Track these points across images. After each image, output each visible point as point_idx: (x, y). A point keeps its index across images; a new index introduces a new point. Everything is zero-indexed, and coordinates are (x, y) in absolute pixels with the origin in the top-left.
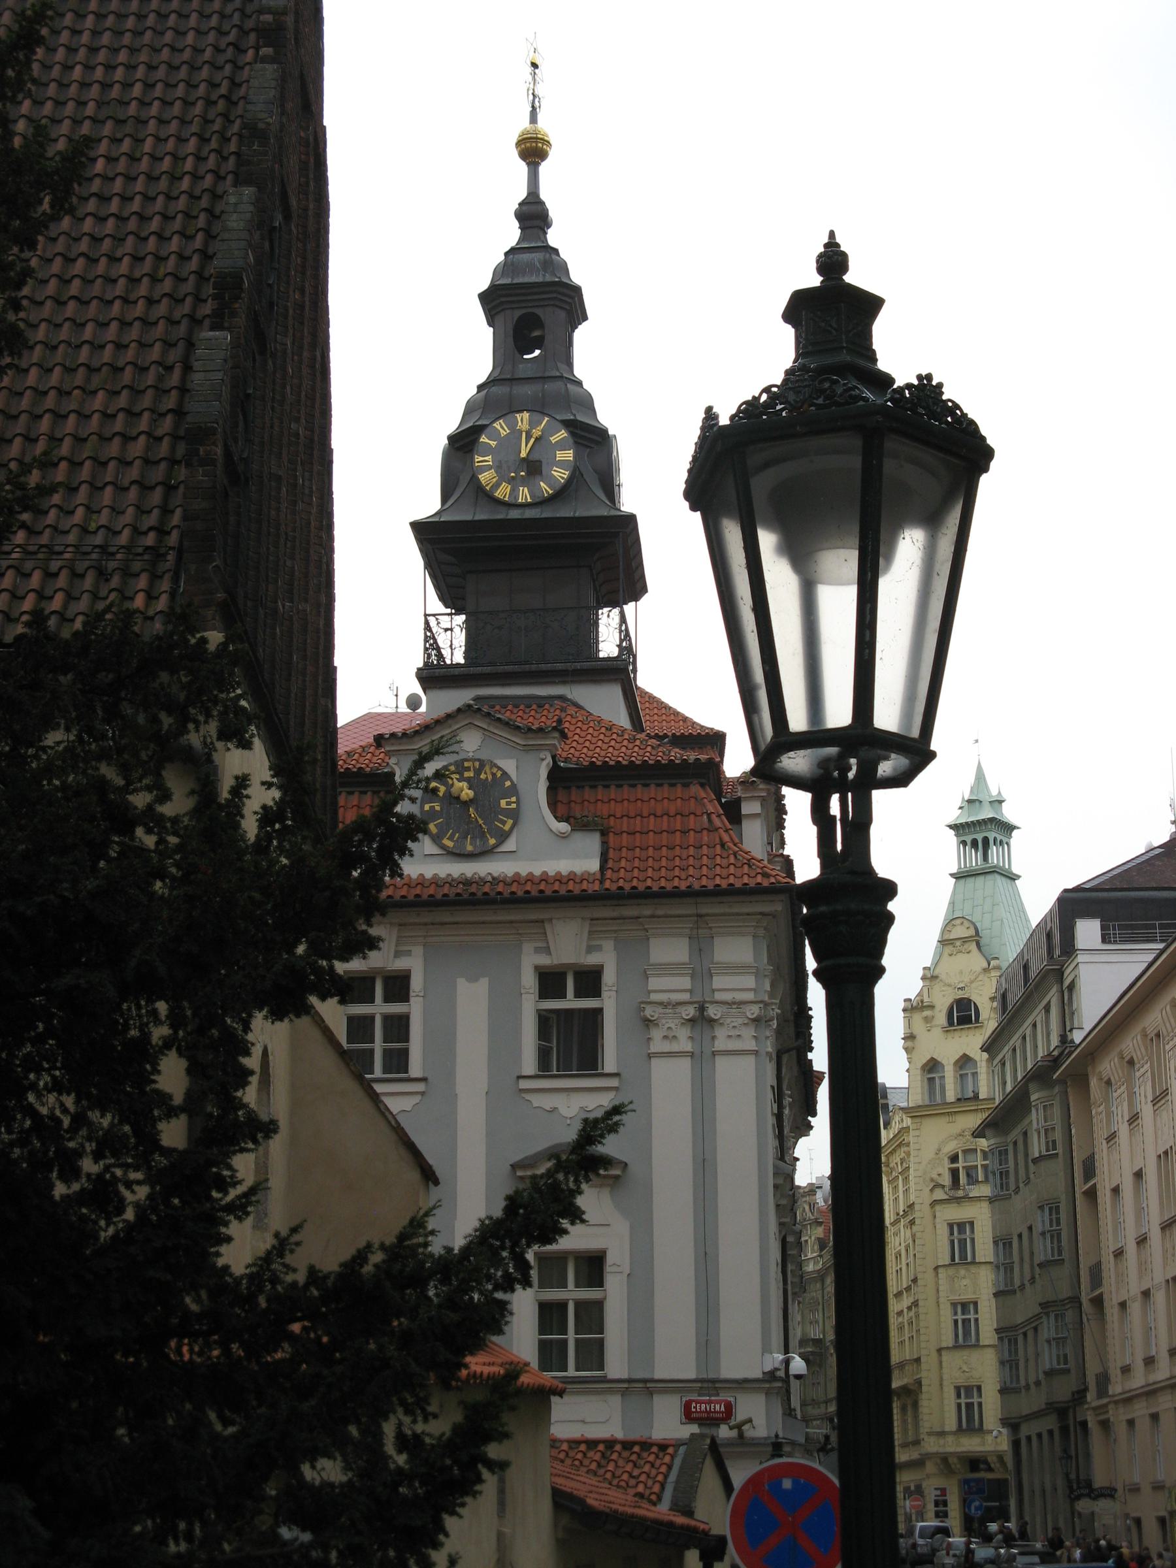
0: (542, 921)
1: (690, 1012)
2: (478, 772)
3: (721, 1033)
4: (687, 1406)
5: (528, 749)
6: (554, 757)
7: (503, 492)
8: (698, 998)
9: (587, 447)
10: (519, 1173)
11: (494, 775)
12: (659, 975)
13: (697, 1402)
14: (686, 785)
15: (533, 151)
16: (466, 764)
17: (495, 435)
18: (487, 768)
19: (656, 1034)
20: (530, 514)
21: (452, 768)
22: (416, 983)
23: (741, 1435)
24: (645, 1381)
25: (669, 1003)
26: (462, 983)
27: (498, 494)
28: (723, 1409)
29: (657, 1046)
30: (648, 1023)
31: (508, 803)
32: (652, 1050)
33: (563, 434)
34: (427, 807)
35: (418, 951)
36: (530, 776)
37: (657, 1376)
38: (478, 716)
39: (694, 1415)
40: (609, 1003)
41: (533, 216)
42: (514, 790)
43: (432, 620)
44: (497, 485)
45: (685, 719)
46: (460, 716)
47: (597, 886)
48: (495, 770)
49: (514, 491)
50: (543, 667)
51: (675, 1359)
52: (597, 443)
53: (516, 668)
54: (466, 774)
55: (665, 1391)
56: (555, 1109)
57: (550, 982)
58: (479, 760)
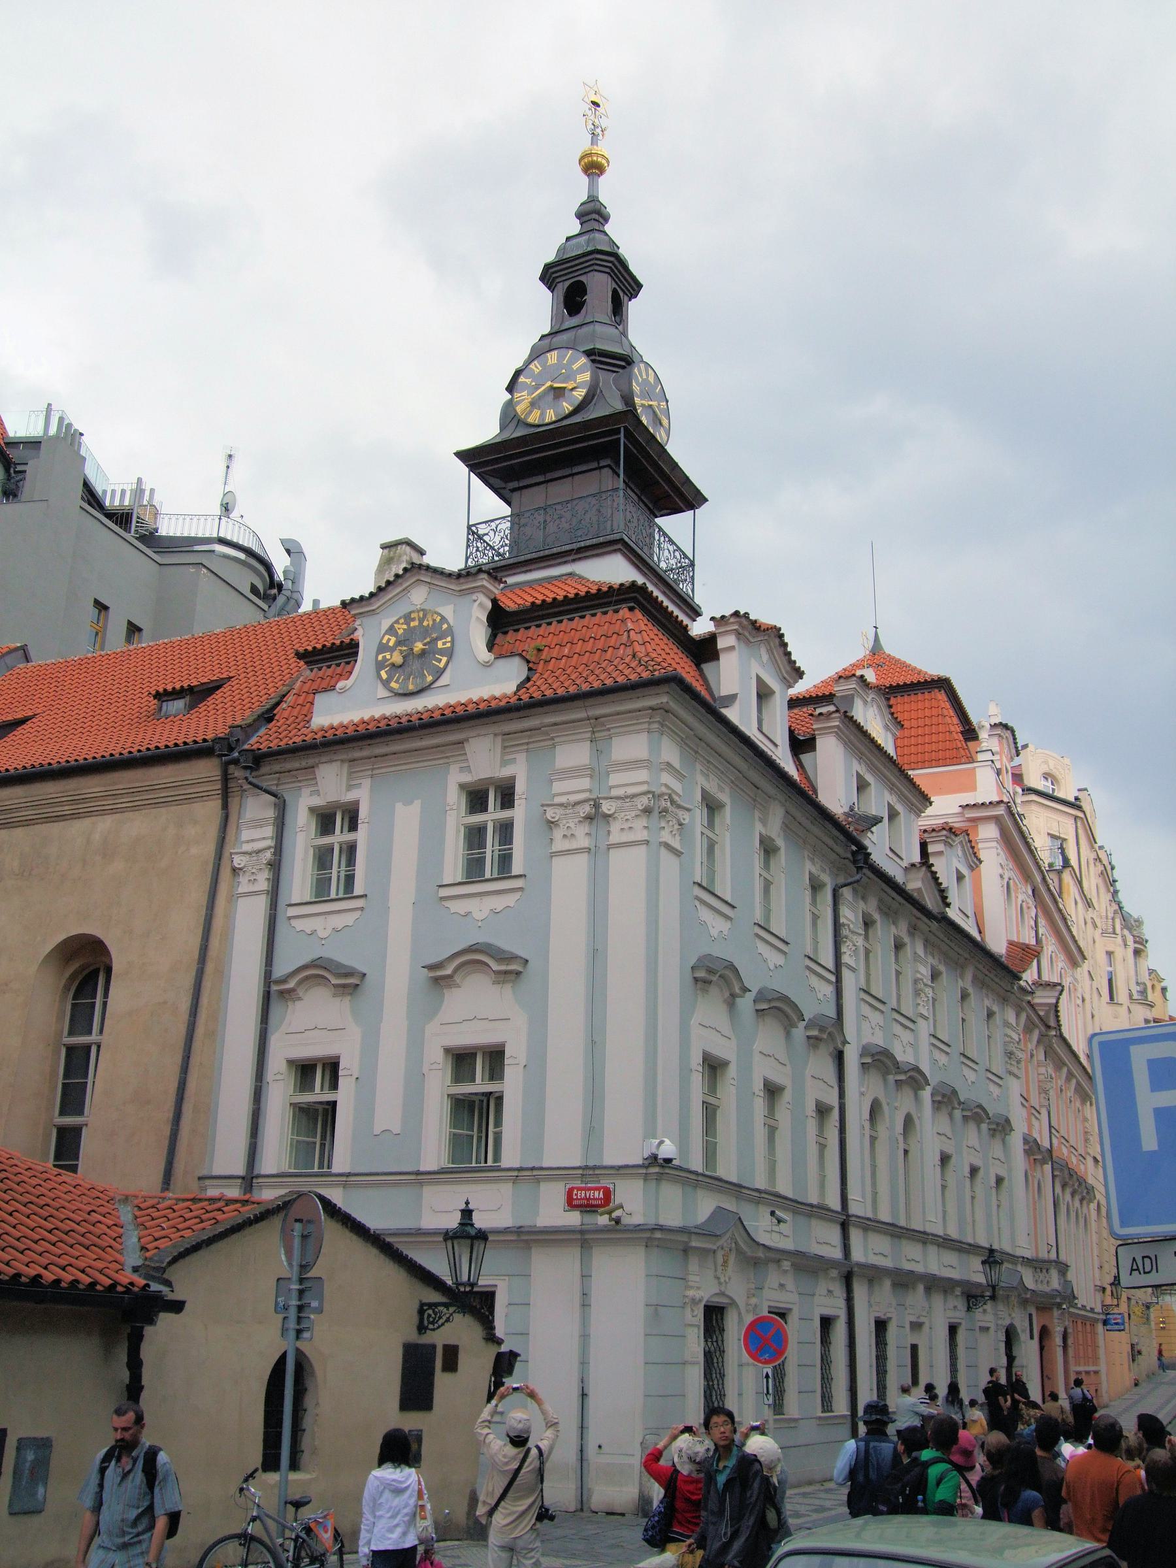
0: (461, 742)
1: (587, 809)
2: (421, 621)
3: (615, 827)
4: (570, 1193)
6: (495, 602)
7: (534, 418)
10: (432, 974)
11: (434, 620)
12: (560, 780)
13: (579, 1189)
14: (616, 611)
15: (593, 168)
16: (413, 616)
17: (532, 375)
19: (558, 834)
21: (402, 621)
22: (363, 814)
23: (618, 1221)
24: (533, 1169)
25: (568, 804)
26: (399, 807)
27: (530, 420)
28: (601, 1196)
29: (559, 844)
30: (551, 824)
31: (444, 644)
32: (554, 850)
33: (583, 360)
34: (380, 657)
36: (470, 621)
37: (544, 1165)
39: (575, 1203)
40: (519, 814)
41: (592, 215)
42: (450, 631)
44: (531, 412)
45: (920, 672)
46: (408, 575)
47: (503, 704)
49: (543, 415)
50: (555, 550)
51: (563, 1149)
52: (623, 367)
53: (534, 556)
54: (412, 624)
55: (550, 1178)
56: (468, 914)
57: (476, 799)
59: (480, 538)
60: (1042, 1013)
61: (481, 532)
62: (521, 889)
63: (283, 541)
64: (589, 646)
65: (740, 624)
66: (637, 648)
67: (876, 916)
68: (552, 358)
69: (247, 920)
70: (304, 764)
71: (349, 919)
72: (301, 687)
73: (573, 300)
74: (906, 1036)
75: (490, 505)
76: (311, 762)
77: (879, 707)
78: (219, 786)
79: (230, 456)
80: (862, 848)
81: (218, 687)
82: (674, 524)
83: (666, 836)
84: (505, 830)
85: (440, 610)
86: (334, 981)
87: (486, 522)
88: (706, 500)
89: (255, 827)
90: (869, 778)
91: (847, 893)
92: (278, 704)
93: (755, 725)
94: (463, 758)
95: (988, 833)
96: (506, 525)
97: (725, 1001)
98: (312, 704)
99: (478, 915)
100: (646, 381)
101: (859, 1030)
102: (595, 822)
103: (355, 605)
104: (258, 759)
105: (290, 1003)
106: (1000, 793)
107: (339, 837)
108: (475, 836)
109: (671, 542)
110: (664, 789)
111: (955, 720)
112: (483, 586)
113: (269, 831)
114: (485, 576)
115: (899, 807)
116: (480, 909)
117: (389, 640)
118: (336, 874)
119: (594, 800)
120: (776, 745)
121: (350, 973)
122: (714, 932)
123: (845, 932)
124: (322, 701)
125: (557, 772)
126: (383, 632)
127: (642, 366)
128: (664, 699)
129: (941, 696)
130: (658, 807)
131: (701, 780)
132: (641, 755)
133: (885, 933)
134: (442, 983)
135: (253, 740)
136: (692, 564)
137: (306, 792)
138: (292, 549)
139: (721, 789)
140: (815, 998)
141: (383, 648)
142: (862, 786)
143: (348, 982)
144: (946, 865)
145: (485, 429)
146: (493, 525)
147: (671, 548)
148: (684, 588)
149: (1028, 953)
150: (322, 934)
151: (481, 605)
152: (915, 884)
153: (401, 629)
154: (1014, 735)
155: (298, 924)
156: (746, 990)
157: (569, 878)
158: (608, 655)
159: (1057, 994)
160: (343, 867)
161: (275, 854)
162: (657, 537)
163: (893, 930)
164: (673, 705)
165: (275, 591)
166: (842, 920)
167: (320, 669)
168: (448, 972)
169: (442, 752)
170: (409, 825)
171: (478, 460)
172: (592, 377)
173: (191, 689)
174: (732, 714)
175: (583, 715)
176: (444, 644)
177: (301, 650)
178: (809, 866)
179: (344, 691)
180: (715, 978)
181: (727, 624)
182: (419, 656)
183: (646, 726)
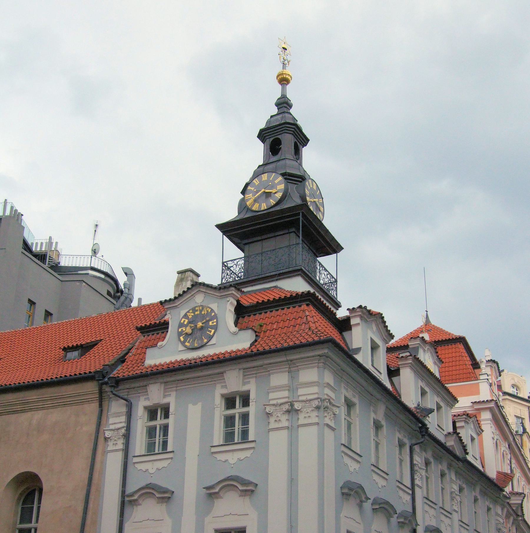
1: (287, 407)
2: (201, 311)
3: (301, 416)
5: (222, 297)
6: (238, 301)
7: (255, 207)
8: (290, 400)
9: (295, 184)
11: (208, 311)
12: (273, 392)
14: (300, 306)
18: (205, 309)
19: (272, 420)
20: (265, 212)
21: (191, 311)
22: (172, 409)
26: (190, 406)
27: (254, 208)
30: (269, 415)
31: (213, 323)
32: (270, 427)
33: (280, 178)
34: (180, 330)
35: (174, 394)
36: (225, 311)
38: (202, 286)
40: (252, 409)
42: (216, 317)
43: (225, 264)
44: (254, 205)
45: (449, 334)
47: (243, 353)
48: (208, 309)
50: (267, 275)
52: (301, 182)
53: (256, 277)
54: (196, 313)
56: (226, 461)
57: (230, 402)
58: (202, 306)
59: (229, 268)
60: (514, 508)
61: (229, 265)
62: (253, 448)
63: (123, 269)
64: (286, 324)
65: (362, 312)
66: (311, 325)
67: (432, 460)
68: (265, 177)
69: (113, 464)
70: (141, 384)
71: (165, 464)
72: (139, 345)
73: (274, 148)
74: (447, 521)
75: (233, 252)
76: (145, 383)
77: (431, 353)
78: (98, 396)
79: (97, 225)
80: (424, 425)
81: (96, 344)
82: (327, 261)
83: (327, 421)
84: (245, 418)
85: (210, 306)
86: (158, 495)
87: (231, 261)
88: (342, 248)
89: (116, 417)
90: (427, 389)
91: (417, 448)
92: (127, 354)
93: (370, 363)
94: (222, 381)
95: (486, 416)
96: (242, 262)
97: (358, 504)
98: (145, 353)
99: (232, 461)
100: (312, 188)
101: (424, 518)
102: (291, 413)
103: (167, 303)
104: (117, 382)
105: (135, 507)
106: (492, 395)
107: (159, 422)
108: (229, 421)
109: (326, 270)
110: (326, 397)
111: (468, 359)
112: (232, 293)
113: (123, 418)
114: (233, 288)
115: (442, 404)
116: (232, 458)
117: (184, 321)
118: (158, 440)
119: (291, 402)
120: (381, 373)
121: (166, 491)
122: (352, 469)
123: (416, 468)
124: (150, 352)
125: (271, 388)
126: (181, 317)
127: (310, 181)
128: (326, 351)
129: (461, 346)
130: (323, 406)
131: (344, 392)
132: (313, 379)
133: (436, 468)
134: (213, 496)
135: (115, 372)
136: (336, 281)
137: (142, 398)
138: (128, 273)
139: (354, 397)
140: (401, 502)
141: (181, 325)
142: (423, 393)
143: (165, 496)
144: (466, 432)
145: (231, 214)
146: (236, 262)
147: (326, 273)
148: (332, 293)
149: (507, 478)
150: (151, 471)
151: (231, 303)
152: (450, 443)
153: (190, 315)
154: (498, 366)
155: (139, 466)
156: (368, 498)
157: (278, 441)
158: (296, 329)
159: (522, 498)
160: (162, 436)
161: (126, 430)
162: (318, 268)
163: (440, 467)
164: (330, 354)
165: (119, 294)
166: (415, 462)
167: (148, 336)
168: (217, 490)
169: (212, 378)
170: (196, 416)
171: (228, 229)
172: (285, 187)
173: (82, 346)
174: (359, 357)
175: (284, 359)
176: (213, 323)
177: (139, 326)
178: (398, 435)
179: (162, 347)
180: (352, 493)
181: (356, 312)
182: (200, 329)
183: (317, 364)
